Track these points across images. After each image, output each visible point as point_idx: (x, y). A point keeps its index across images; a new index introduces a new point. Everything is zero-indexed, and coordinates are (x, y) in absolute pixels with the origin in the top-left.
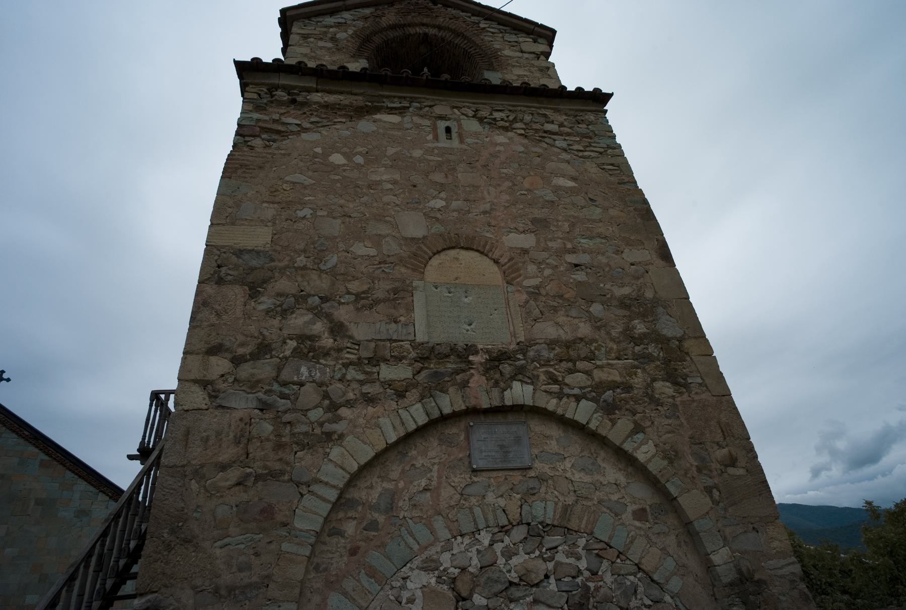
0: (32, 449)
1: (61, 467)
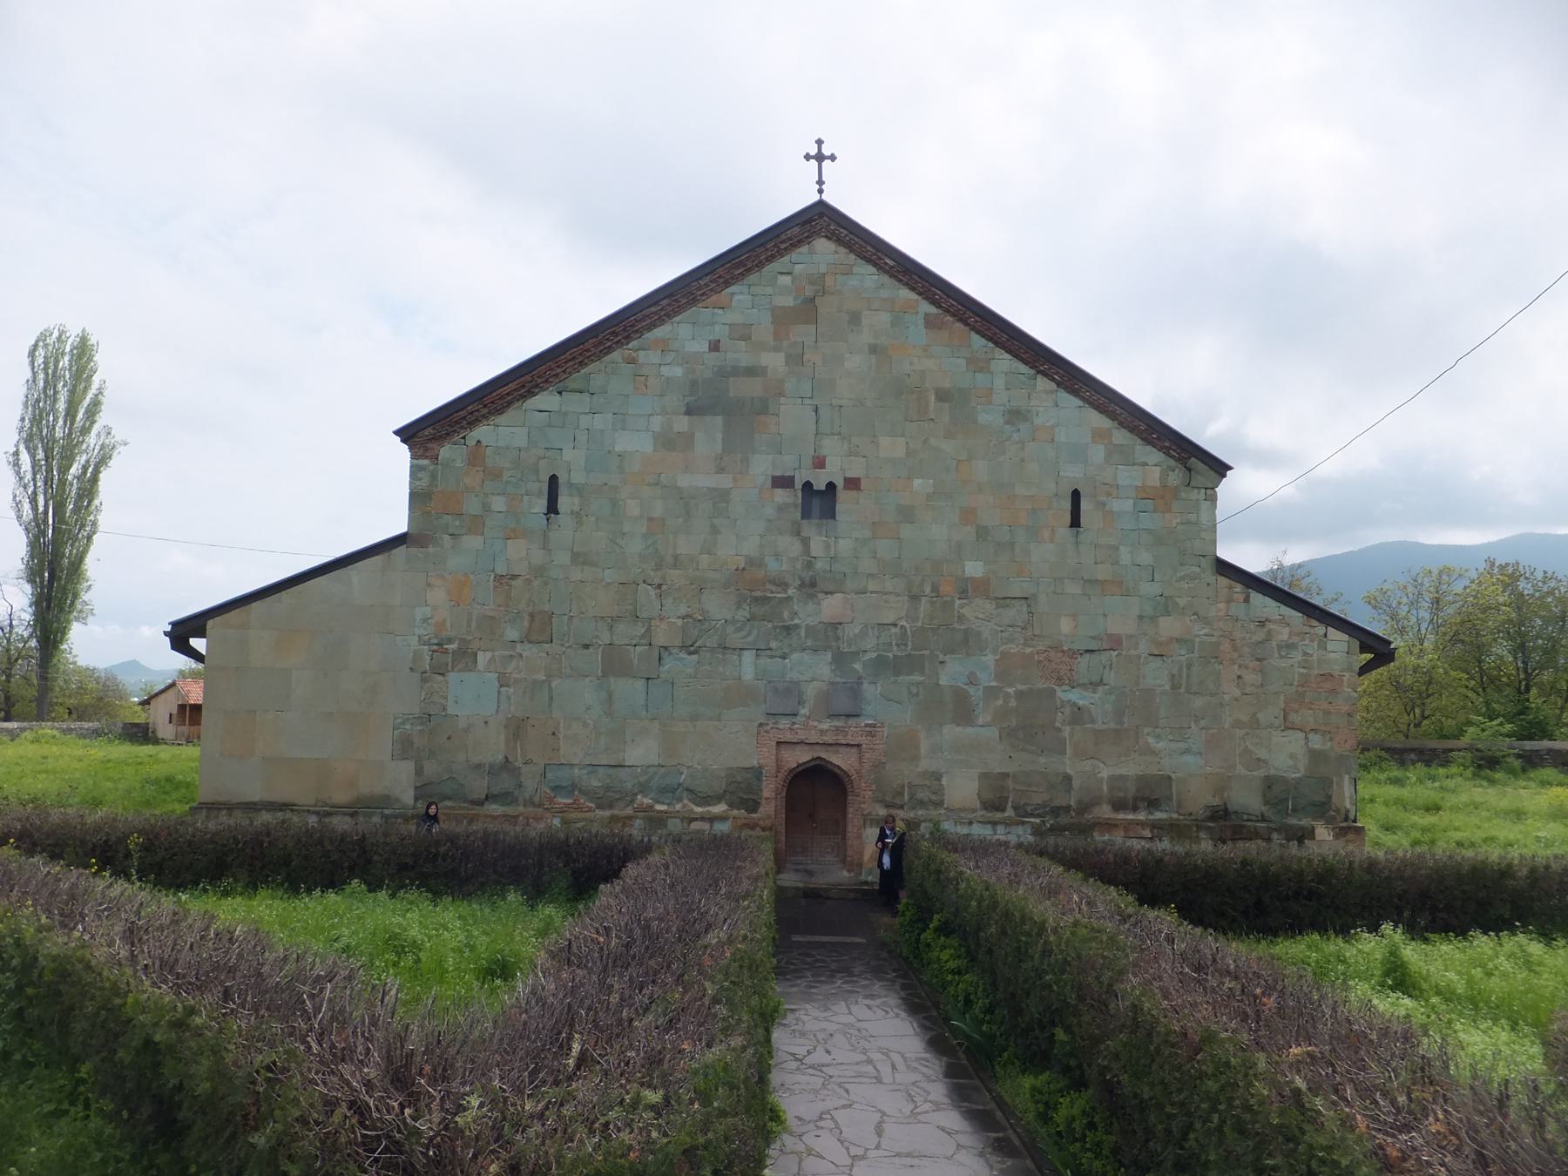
0: (905, 294)
1: (959, 325)
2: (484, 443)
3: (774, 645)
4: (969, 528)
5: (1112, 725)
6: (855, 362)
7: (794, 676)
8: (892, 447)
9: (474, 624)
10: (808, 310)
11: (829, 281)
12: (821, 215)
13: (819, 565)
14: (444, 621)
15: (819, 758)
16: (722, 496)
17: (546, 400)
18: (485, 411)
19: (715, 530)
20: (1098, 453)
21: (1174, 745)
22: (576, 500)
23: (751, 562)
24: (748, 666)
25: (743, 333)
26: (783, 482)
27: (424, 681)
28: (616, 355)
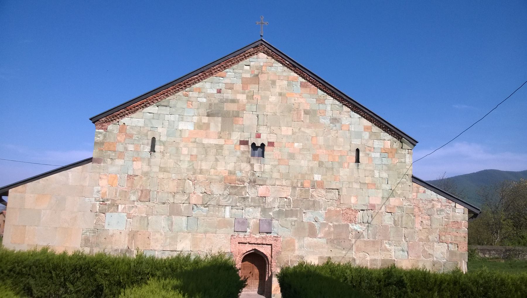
2: (126, 124)
3: (238, 204)
4: (316, 162)
5: (371, 239)
6: (273, 99)
7: (247, 217)
8: (286, 131)
9: (118, 194)
10: (256, 78)
11: (264, 69)
12: (262, 44)
13: (257, 175)
14: (106, 192)
15: (255, 249)
16: (221, 147)
17: (152, 109)
18: (127, 112)
19: (217, 160)
20: (366, 135)
21: (396, 248)
22: (162, 147)
23: (230, 173)
24: (227, 212)
25: (230, 87)
26: (244, 143)
27: (96, 215)
28: (180, 93)
